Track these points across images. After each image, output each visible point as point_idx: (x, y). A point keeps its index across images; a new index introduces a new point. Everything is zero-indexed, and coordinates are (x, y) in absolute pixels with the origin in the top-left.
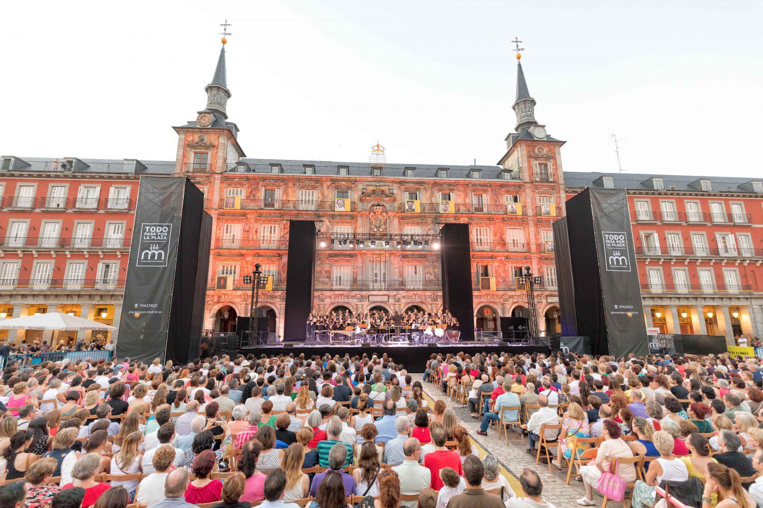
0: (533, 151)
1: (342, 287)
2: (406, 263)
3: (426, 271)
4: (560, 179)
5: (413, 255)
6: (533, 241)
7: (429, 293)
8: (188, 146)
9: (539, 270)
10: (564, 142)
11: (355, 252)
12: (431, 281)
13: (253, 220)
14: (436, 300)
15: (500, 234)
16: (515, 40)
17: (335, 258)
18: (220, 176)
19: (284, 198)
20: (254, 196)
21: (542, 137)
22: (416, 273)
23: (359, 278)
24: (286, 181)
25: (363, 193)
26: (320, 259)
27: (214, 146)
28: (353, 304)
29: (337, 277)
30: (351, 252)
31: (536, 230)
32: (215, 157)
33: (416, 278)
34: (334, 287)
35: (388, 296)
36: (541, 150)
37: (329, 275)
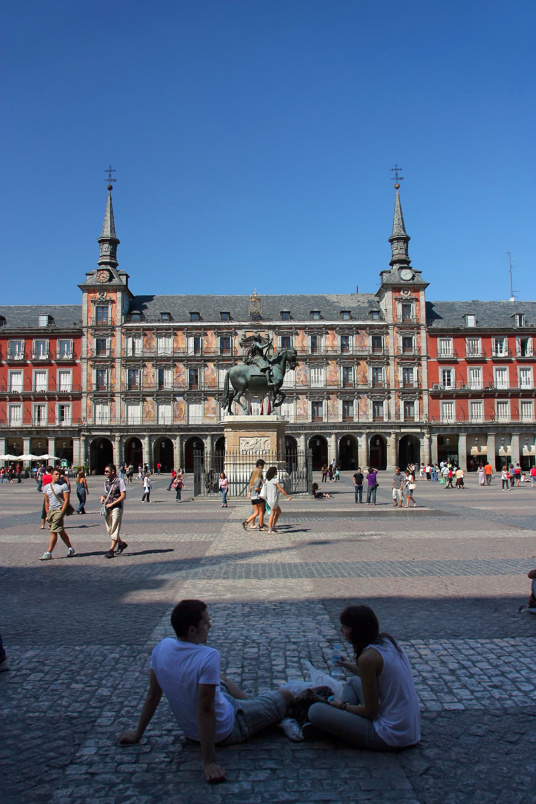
6: (392, 378)
9: (396, 404)
15: (364, 372)
16: (394, 168)
19: (175, 346)
20: (149, 344)
27: (113, 302)
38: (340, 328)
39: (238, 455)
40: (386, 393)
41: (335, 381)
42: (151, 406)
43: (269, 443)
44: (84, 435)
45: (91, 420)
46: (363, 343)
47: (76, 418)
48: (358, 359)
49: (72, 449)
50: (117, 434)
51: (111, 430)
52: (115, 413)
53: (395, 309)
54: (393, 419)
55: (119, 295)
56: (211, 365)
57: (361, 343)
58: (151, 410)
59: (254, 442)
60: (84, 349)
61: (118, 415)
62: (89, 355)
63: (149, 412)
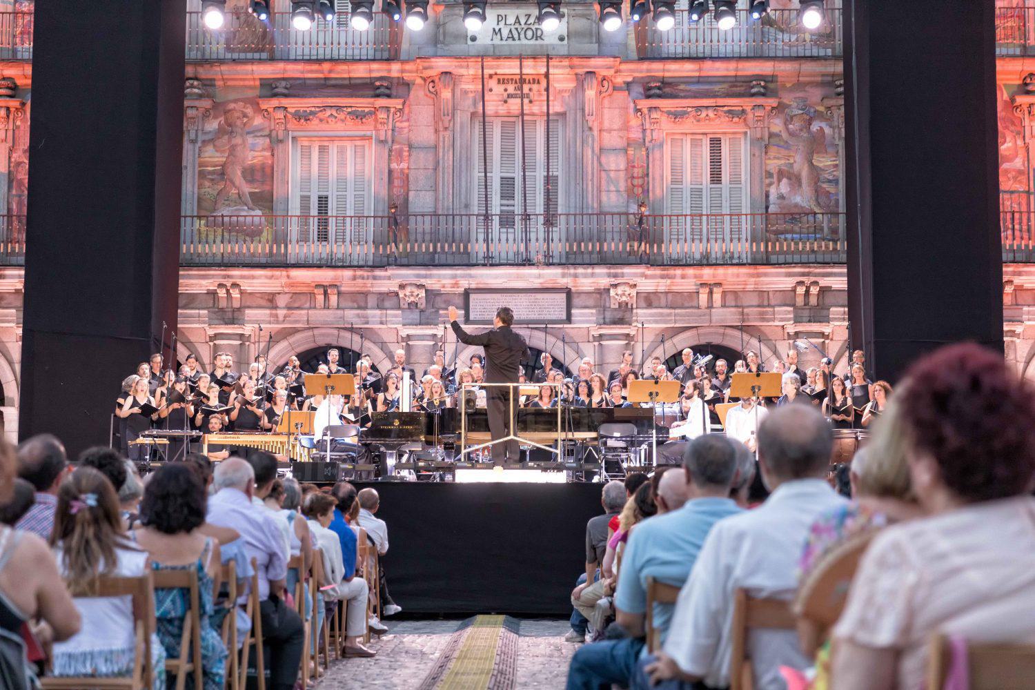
1: (339, 250)
2: (666, 125)
3: (773, 164)
5: (700, 80)
7: (779, 280)
11: (395, 69)
12: (793, 216)
14: (818, 313)
17: (293, 104)
22: (716, 177)
23: (421, 201)
26: (218, 108)
28: (389, 337)
29: (305, 200)
30: (378, 70)
33: (716, 202)
34: (295, 251)
35: (569, 293)
37: (264, 178)
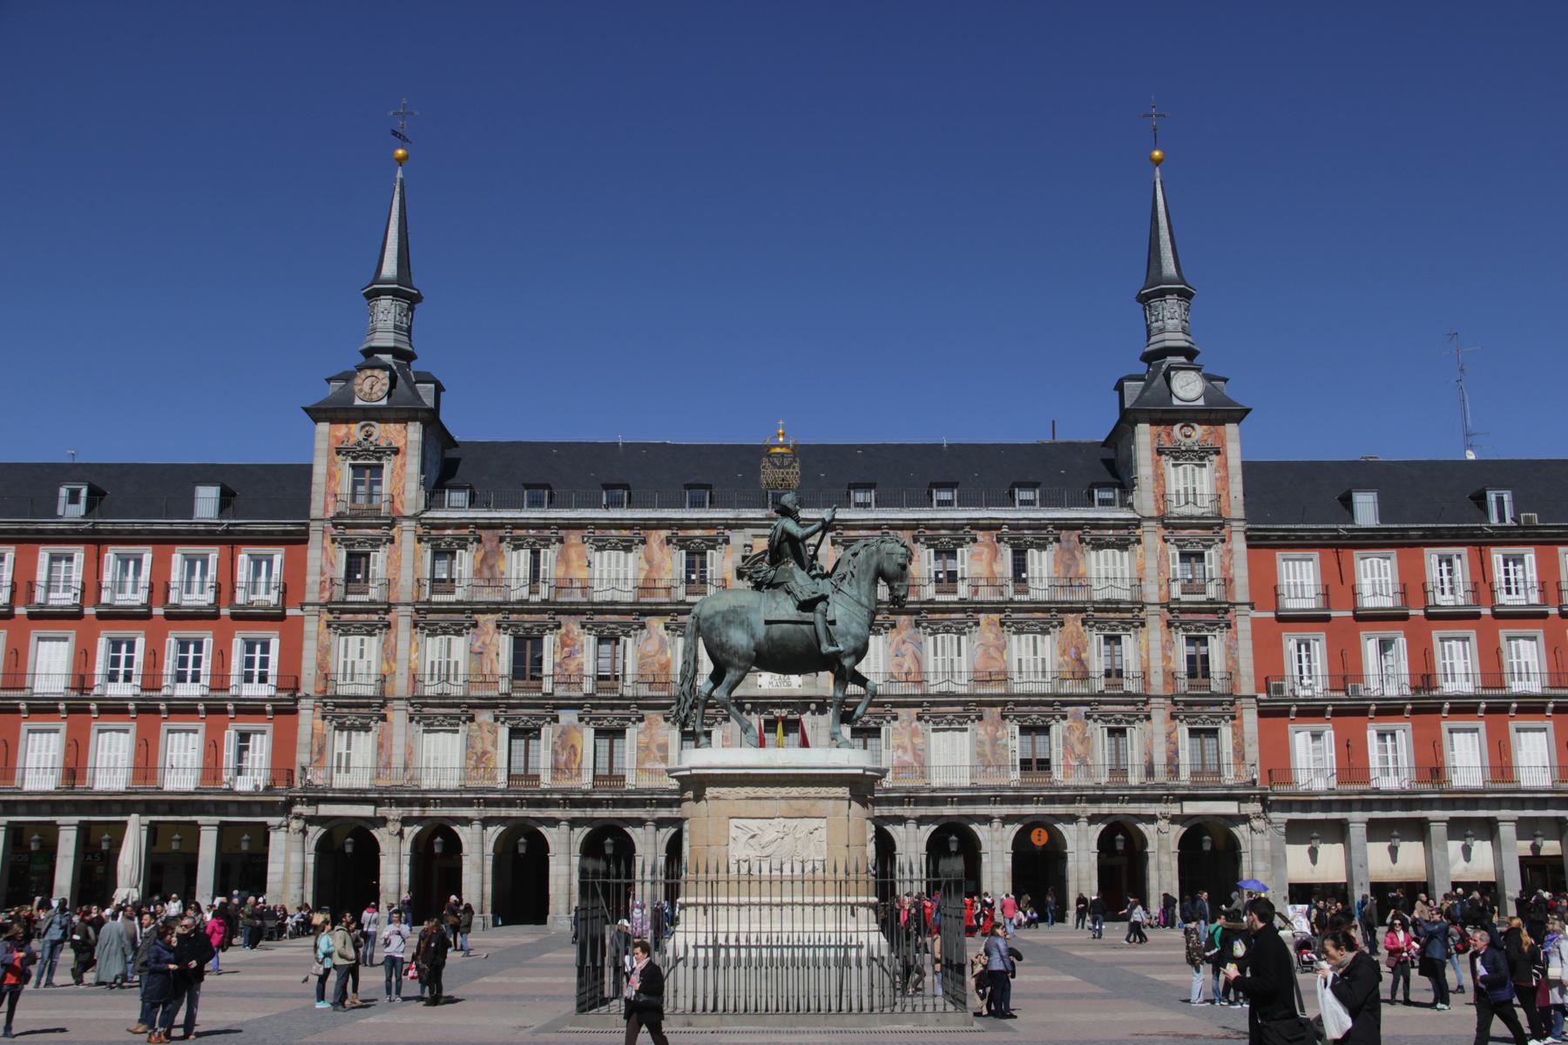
0: (1169, 435)
4: (1233, 503)
6: (1157, 665)
8: (338, 453)
9: (1169, 735)
10: (1247, 411)
13: (492, 626)
15: (1077, 648)
18: (413, 523)
20: (491, 568)
21: (1193, 395)
24: (562, 533)
25: (744, 558)
27: (396, 451)
31: (1165, 637)
32: (398, 476)
36: (1187, 430)
38: (1011, 527)
39: (722, 875)
40: (1139, 706)
41: (998, 673)
42: (488, 737)
43: (824, 837)
44: (298, 817)
45: (321, 774)
46: (1073, 570)
47: (283, 766)
48: (1060, 611)
49: (266, 856)
50: (394, 813)
51: (377, 803)
52: (390, 757)
53: (1159, 477)
54: (1161, 776)
55: (414, 432)
56: (657, 624)
57: (1068, 568)
58: (490, 749)
59: (775, 835)
60: (313, 579)
61: (398, 761)
62: (327, 595)
63: (484, 753)
